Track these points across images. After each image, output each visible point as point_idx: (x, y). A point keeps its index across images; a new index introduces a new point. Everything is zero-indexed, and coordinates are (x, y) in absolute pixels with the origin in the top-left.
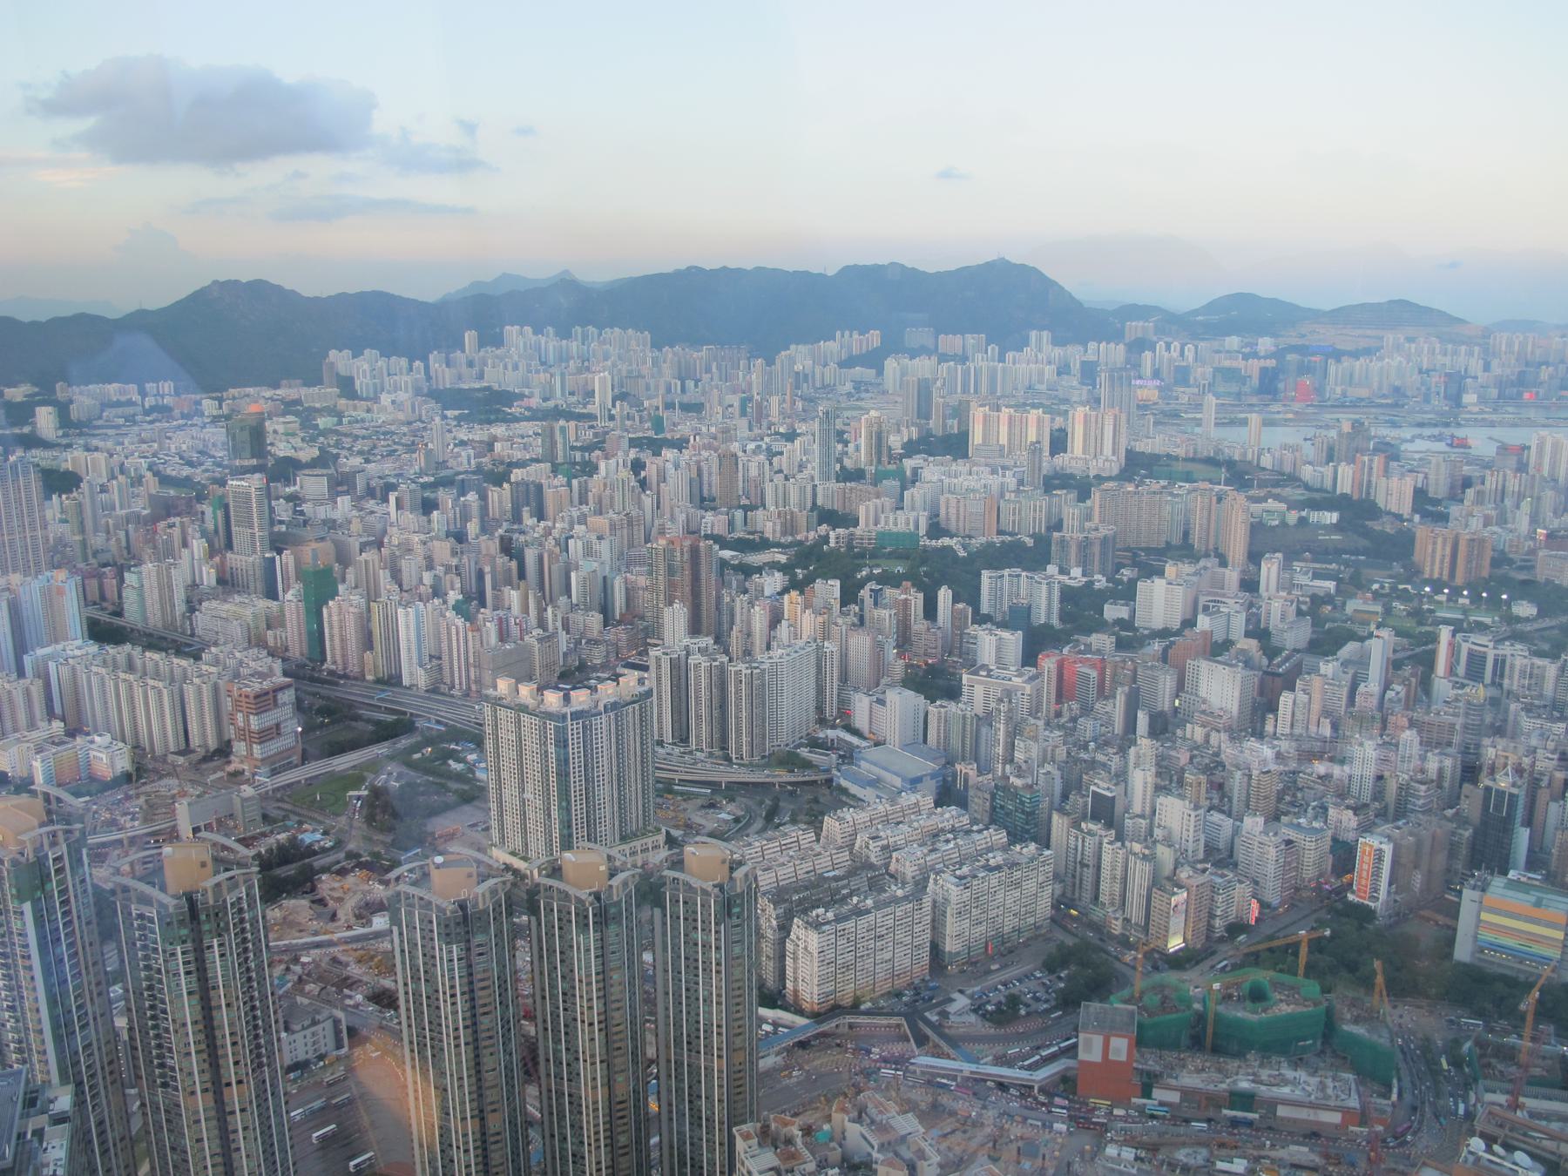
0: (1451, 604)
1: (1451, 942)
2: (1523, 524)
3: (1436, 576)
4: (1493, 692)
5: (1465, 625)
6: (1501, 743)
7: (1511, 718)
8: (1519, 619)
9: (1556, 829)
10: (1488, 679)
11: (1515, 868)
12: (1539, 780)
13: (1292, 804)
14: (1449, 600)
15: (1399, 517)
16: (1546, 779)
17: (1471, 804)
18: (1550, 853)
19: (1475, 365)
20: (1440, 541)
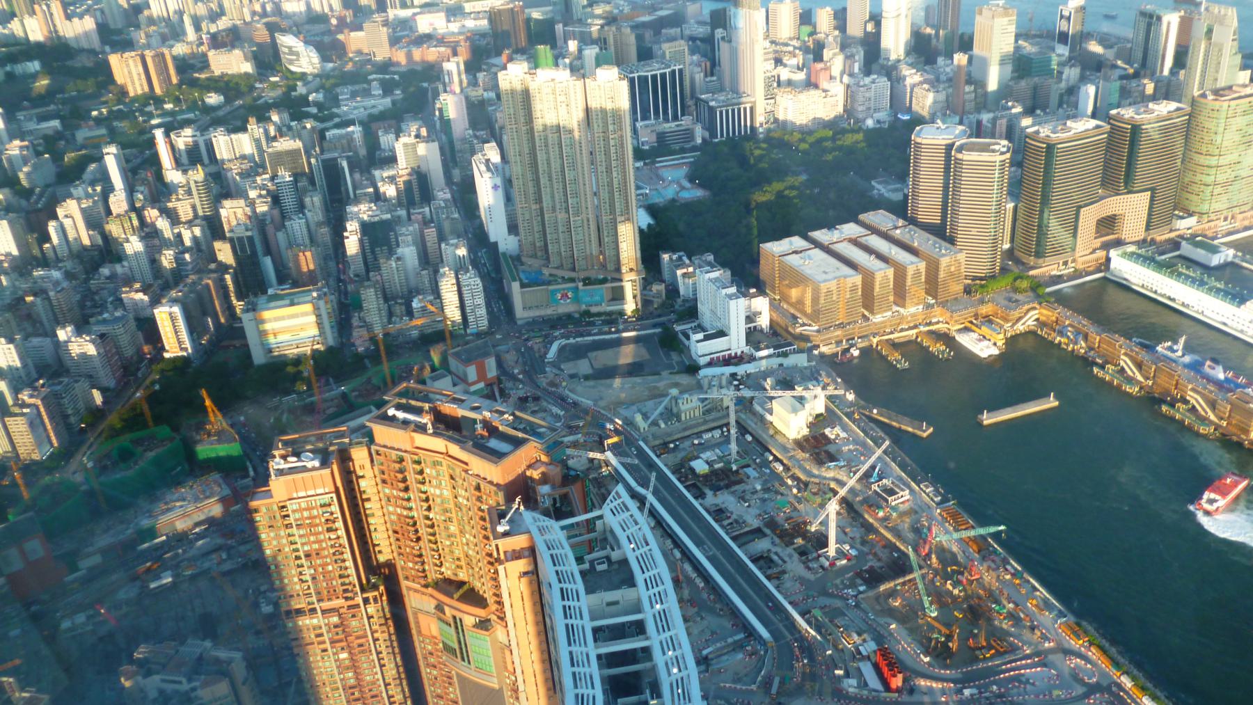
0: (159, 112)
1: (248, 355)
2: (191, 35)
3: (140, 92)
4: (213, 169)
6: (227, 203)
8: (213, 109)
10: (206, 160)
11: (271, 286)
12: (264, 220)
13: (95, 306)
15: (92, 52)
16: (268, 218)
17: (224, 253)
18: (290, 269)
20: (131, 62)
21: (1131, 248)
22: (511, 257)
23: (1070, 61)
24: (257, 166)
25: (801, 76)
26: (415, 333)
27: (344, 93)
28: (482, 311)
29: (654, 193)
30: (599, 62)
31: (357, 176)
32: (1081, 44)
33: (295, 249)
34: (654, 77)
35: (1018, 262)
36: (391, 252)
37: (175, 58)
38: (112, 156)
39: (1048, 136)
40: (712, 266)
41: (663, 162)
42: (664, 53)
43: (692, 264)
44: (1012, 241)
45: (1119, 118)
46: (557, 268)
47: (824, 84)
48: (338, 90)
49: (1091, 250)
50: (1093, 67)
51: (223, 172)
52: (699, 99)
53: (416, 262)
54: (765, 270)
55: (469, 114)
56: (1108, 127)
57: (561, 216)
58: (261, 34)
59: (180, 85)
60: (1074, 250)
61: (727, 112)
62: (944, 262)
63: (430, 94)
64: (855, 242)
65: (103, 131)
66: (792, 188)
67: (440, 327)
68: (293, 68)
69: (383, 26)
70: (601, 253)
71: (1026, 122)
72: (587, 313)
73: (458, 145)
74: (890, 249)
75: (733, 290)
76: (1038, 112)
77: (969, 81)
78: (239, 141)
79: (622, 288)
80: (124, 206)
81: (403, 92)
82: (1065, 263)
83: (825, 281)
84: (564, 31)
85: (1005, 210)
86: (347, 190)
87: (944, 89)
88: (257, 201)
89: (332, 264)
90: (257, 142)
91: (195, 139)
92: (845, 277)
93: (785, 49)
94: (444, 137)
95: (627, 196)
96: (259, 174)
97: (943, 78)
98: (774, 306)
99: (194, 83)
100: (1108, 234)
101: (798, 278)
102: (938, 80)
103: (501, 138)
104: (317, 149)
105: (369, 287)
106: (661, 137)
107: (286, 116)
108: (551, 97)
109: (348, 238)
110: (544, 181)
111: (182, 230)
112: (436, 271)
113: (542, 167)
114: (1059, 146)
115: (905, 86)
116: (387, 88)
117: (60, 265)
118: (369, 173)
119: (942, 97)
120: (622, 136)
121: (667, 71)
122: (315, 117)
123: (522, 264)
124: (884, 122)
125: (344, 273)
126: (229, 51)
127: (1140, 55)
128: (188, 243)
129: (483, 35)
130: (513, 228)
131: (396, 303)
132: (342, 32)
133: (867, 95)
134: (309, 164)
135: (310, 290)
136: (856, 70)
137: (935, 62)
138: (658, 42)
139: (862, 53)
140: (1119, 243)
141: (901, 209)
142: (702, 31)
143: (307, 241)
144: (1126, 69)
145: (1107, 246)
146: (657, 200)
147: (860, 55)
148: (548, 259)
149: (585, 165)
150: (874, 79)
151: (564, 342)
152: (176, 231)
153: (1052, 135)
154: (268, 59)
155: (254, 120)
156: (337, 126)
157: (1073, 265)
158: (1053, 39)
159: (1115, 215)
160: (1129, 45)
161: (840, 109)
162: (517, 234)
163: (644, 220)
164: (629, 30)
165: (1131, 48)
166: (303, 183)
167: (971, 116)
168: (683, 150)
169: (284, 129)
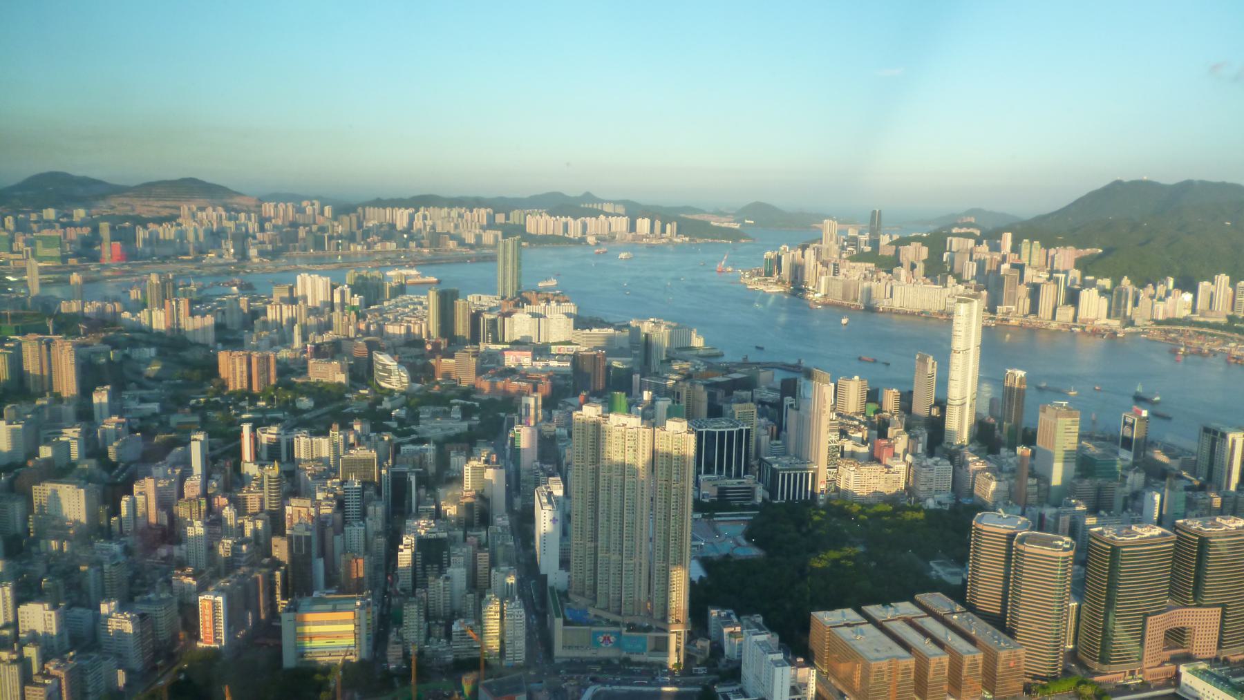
0: (251, 408)
1: (279, 656)
2: (297, 342)
3: (238, 387)
4: (288, 467)
5: (264, 422)
6: (294, 502)
7: (302, 484)
9: (341, 554)
10: (284, 458)
12: (326, 522)
13: (143, 585)
14: (250, 404)
15: (205, 346)
17: (280, 549)
19: (253, 226)
20: (237, 360)
21: (1203, 666)
22: (558, 592)
23: (1135, 466)
24: (331, 469)
25: (864, 450)
26: (450, 657)
27: (425, 412)
28: (521, 644)
29: (708, 545)
30: (672, 414)
31: (422, 492)
32: (1145, 451)
33: (349, 556)
34: (721, 434)
35: (1082, 665)
36: (441, 570)
37: (278, 362)
38: (198, 444)
39: (1113, 538)
40: (761, 628)
41: (722, 517)
42: (733, 413)
43: (740, 623)
44: (1075, 642)
45: (1182, 528)
46: (603, 609)
47: (888, 461)
48: (421, 409)
49: (1159, 662)
50: (1157, 475)
51: (297, 471)
52: (762, 461)
53: (465, 584)
54: (815, 640)
55: (539, 447)
56: (1174, 537)
57: (615, 557)
58: (360, 349)
59: (276, 387)
60: (1140, 660)
61: (789, 476)
62: (1003, 655)
63: (505, 423)
64: (910, 622)
65: (196, 418)
66: (848, 558)
67: (476, 654)
68: (383, 384)
69: (473, 356)
70: (649, 600)
71: (1090, 521)
72: (627, 661)
73: (524, 475)
74: (946, 634)
75: (780, 656)
76: (1102, 512)
77: (1032, 474)
78: (319, 444)
79: (666, 640)
80: (198, 491)
81: (481, 418)
82: (1132, 673)
83: (877, 659)
84: (641, 381)
85: (1068, 608)
86: (410, 503)
87: (1007, 479)
88: (323, 503)
89: (381, 575)
90: (335, 446)
91: (278, 437)
92: (899, 658)
93: (850, 422)
94: (512, 466)
95: (682, 546)
96: (330, 478)
97: (1006, 468)
98: (820, 679)
99: (289, 386)
100: (1177, 647)
101: (849, 654)
102: (1001, 470)
103: (567, 473)
104: (390, 461)
105: (412, 603)
106: (722, 491)
107: (367, 426)
108: (621, 441)
109: (402, 550)
110: (602, 519)
111: (246, 521)
112: (482, 596)
113: (602, 507)
114: (1124, 550)
115: (968, 471)
116: (467, 412)
117: (122, 539)
118: (434, 490)
119: (1004, 486)
120: (684, 487)
121: (735, 430)
122: (394, 431)
123: (569, 600)
124: (945, 504)
125: (391, 585)
126: (330, 361)
127: (1205, 471)
128: (248, 533)
129: (565, 376)
130: (565, 563)
131: (437, 623)
132: (434, 358)
133: (929, 475)
134: (380, 474)
135: (354, 598)
136: (920, 450)
137: (999, 453)
138: (729, 402)
139: (926, 435)
140: (1188, 658)
141: (958, 594)
142: (771, 396)
143: (362, 548)
144: (1191, 481)
145: (1176, 660)
146: (714, 554)
147: (924, 436)
148: (595, 599)
149: (644, 511)
150: (937, 462)
151: (599, 688)
152: (240, 521)
153: (1116, 537)
154: (362, 373)
155: (337, 426)
156: (414, 442)
157: (1140, 676)
158: (1117, 443)
159: (1184, 628)
160: (1194, 458)
161: (902, 485)
162: (568, 569)
163: (698, 572)
164: (702, 388)
165: (1196, 461)
166: (370, 492)
167: (1034, 509)
168: (743, 508)
169: (363, 439)
